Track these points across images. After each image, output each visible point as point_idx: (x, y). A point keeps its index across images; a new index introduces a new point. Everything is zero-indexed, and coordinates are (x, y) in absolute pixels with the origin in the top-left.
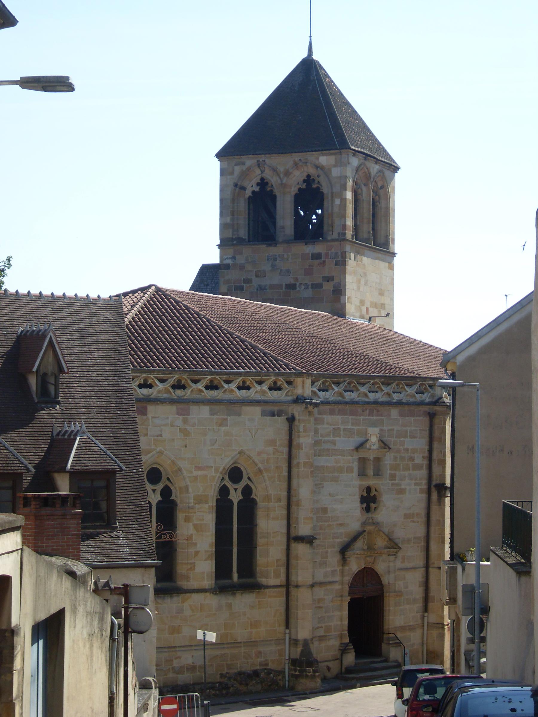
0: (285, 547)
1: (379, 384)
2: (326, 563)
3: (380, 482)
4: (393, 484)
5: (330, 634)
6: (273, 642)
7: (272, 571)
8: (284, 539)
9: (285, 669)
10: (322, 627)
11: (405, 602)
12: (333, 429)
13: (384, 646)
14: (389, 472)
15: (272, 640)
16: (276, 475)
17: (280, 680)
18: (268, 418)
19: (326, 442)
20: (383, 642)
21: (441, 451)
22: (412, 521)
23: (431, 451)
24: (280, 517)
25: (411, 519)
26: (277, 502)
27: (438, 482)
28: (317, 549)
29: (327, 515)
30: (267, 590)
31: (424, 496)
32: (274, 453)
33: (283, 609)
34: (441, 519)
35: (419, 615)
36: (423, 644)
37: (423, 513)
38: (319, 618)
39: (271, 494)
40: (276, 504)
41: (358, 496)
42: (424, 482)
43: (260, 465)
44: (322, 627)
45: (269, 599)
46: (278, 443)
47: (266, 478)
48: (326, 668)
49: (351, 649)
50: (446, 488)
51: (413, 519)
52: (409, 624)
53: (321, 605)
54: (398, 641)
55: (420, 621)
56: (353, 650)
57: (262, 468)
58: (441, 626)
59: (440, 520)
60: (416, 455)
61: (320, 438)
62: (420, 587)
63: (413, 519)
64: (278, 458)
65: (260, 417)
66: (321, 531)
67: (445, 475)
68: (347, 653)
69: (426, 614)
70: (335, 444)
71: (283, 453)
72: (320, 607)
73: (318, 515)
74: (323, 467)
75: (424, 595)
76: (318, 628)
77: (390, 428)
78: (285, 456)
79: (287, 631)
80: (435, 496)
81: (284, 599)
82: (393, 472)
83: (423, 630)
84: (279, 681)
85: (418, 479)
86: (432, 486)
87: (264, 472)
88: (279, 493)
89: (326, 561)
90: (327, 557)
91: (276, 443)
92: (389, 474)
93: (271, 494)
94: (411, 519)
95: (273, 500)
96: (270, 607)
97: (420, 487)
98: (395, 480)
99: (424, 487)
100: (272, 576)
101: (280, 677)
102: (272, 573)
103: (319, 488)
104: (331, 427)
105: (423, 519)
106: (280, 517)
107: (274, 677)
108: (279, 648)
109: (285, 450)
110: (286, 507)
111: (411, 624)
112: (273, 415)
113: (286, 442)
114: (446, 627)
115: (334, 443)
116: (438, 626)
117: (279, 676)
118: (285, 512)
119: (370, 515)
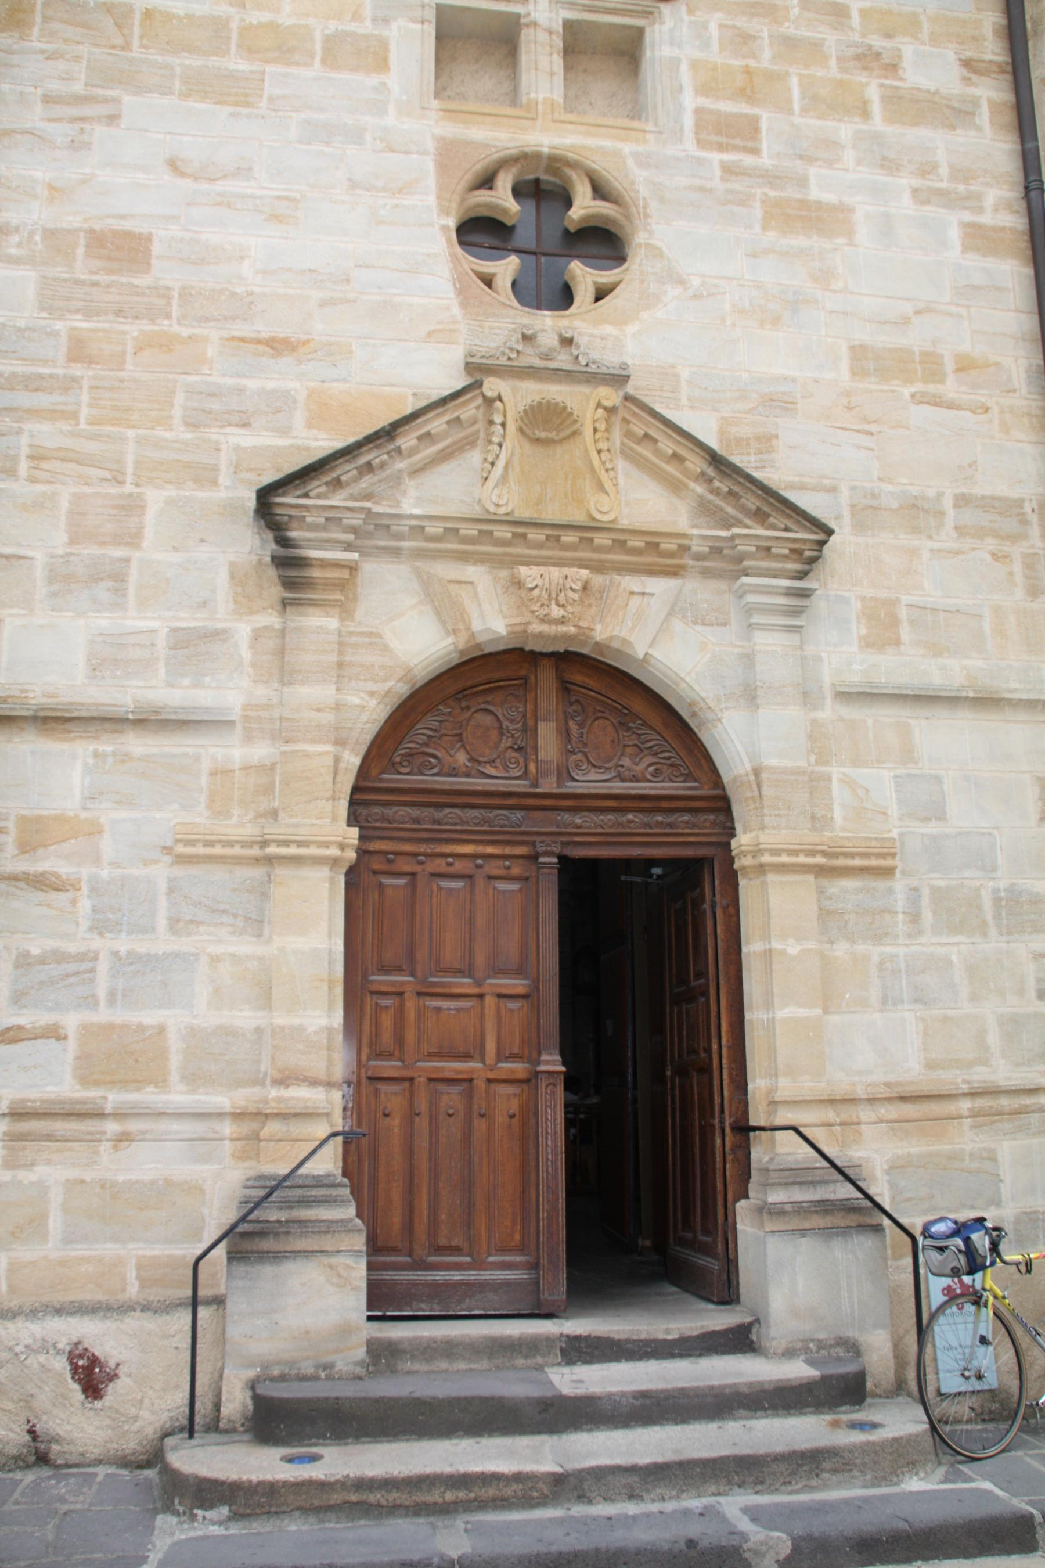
2: (118, 578)
3: (627, 148)
4: (728, 170)
5: (149, 1096)
10: (55, 1033)
11: (927, 916)
14: (690, 101)
22: (937, 402)
25: (918, 387)
28: (32, 480)
29: (142, 281)
41: (432, 200)
44: (55, 1033)
48: (61, 1365)
49: (329, 1228)
51: (931, 388)
54: (845, 1191)
56: (360, 1242)
63: (931, 388)
66: (78, 370)
68: (277, 1257)
73: (60, 271)
82: (727, 107)
85: (944, 171)
89: (127, 560)
90: (133, 539)
92: (698, 111)
94: (918, 387)
97: (968, 217)
98: (755, 151)
103: (82, 119)
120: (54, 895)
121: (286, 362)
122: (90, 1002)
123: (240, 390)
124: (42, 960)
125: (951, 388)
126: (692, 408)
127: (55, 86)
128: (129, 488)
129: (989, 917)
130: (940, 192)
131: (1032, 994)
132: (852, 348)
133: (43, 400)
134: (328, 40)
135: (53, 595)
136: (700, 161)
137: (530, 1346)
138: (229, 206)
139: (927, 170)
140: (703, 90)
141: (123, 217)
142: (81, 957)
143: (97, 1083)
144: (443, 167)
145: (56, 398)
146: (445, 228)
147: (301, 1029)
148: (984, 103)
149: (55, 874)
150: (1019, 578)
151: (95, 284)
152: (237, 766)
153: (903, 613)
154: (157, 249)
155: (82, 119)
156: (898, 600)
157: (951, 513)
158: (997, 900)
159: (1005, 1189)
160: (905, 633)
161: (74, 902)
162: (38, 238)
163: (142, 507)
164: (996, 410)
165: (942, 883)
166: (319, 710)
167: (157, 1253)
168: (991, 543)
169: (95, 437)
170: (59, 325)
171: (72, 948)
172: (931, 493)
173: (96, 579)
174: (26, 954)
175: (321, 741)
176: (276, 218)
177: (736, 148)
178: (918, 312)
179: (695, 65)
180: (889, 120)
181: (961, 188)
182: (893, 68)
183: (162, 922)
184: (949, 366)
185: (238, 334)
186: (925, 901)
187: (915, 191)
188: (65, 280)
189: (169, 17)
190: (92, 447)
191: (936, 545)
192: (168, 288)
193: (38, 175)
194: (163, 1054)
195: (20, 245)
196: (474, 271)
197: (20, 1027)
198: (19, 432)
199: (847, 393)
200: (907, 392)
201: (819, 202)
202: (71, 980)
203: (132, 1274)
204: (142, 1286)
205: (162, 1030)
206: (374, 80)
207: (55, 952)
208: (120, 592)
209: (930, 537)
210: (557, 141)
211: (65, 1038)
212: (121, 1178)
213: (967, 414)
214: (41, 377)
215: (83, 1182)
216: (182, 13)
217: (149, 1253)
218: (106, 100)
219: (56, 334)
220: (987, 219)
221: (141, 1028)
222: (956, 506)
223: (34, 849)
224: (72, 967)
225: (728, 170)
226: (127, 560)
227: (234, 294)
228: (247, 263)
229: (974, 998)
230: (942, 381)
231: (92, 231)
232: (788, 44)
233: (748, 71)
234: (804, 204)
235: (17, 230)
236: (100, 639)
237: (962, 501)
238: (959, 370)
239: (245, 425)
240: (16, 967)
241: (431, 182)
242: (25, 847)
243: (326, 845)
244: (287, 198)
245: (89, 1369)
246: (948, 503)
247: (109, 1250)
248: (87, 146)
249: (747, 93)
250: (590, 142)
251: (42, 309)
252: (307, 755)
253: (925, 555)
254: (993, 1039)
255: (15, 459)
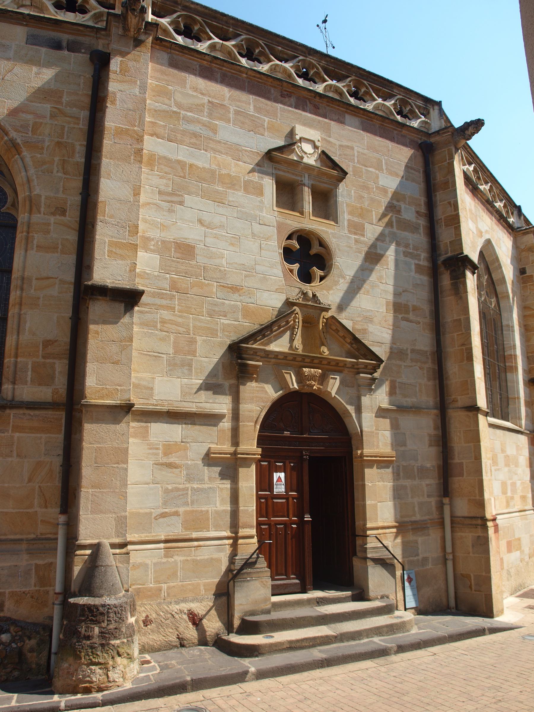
0: (69, 313)
1: (318, 69)
2: (190, 365)
3: (330, 231)
6: (24, 546)
7: (30, 366)
8: (69, 296)
9: (51, 618)
10: (176, 514)
11: (401, 474)
12: (209, 101)
13: (356, 562)
15: (22, 540)
16: (56, 159)
17: (31, 650)
18: (44, 50)
19: (189, 121)
20: (355, 554)
21: (449, 203)
22: (407, 320)
23: (430, 205)
24: (60, 247)
25: (403, 315)
26: (53, 214)
27: (449, 254)
30: (12, 413)
31: (425, 279)
32: (53, 116)
33: (57, 462)
34: (462, 317)
35: (433, 501)
36: (445, 560)
37: (426, 308)
38: (167, 491)
39: (39, 196)
40: (52, 219)
42: (424, 255)
43: (13, 134)
44: (176, 514)
45: (17, 435)
46: (65, 99)
47: (28, 160)
48: (185, 617)
50: (466, 261)
51: (406, 316)
52: (413, 519)
53: (172, 459)
55: (435, 515)
57: (19, 141)
58: (479, 522)
59: (460, 320)
60: (403, 206)
61: (175, 109)
62: (430, 445)
63: (406, 316)
64: (64, 127)
65: (23, 44)
67: (461, 240)
69: (446, 500)
70: (216, 134)
71: (78, 119)
72: (170, 466)
74: (179, 162)
75: (441, 463)
76: (163, 515)
77: (345, 143)
78: (83, 125)
79: (62, 519)
80: (446, 280)
81: (61, 437)
82: (356, 219)
83: (444, 532)
84: (29, 655)
85: (411, 246)
86: (439, 262)
87: (24, 149)
88: (61, 195)
89: (192, 360)
90: (193, 353)
91: (61, 97)
93: (39, 196)
95: (42, 209)
96: (18, 456)
97: (417, 262)
98: (363, 236)
99: (425, 263)
100: (29, 379)
101: (31, 643)
102: (29, 373)
103: (172, 202)
104: (206, 99)
105: (426, 319)
106: (60, 247)
107: (13, 640)
108: (41, 562)
109: (84, 114)
110: (77, 226)
111: (418, 517)
112: (57, 46)
113: (87, 101)
114: (490, 524)
115: (215, 130)
116: (474, 522)
117: (30, 638)
118: (73, 237)
119: (309, 289)
120: (174, 470)
121: (236, 296)
122: (186, 504)
123: (224, 304)
124: (172, 491)
125: (411, 316)
126: (346, 319)
127: (162, 188)
128: (192, 336)
129: (416, 474)
130: (410, 253)
131: (426, 496)
132: (387, 302)
133: (164, 302)
134: (245, 182)
135: (171, 370)
136: (349, 237)
137: (309, 602)
138: (218, 239)
139: (407, 246)
140: (350, 213)
141: (186, 239)
142: (183, 489)
143: (189, 529)
144: (279, 232)
145: (168, 302)
146: (279, 253)
147: (247, 510)
148: (421, 225)
149: (175, 463)
150: (425, 375)
151: (178, 262)
152: (226, 429)
153: (397, 384)
154: (197, 251)
155: (172, 202)
156: (396, 381)
157: (410, 354)
158: (418, 469)
159: (420, 551)
160: (398, 392)
161: (181, 472)
162: (160, 243)
163: (196, 342)
164: (422, 323)
165: (405, 464)
166: (250, 412)
167: (209, 581)
168: (419, 364)
169: (180, 317)
170: (168, 276)
171: (181, 486)
172: (405, 348)
173: (183, 365)
174: (167, 489)
175: (251, 422)
176: (232, 244)
177: (359, 234)
178: (403, 291)
179: (347, 205)
180: (398, 229)
181: (415, 252)
182: (399, 212)
183: (206, 478)
184: (411, 309)
185: (222, 284)
186: (401, 469)
187: (404, 252)
188: (169, 260)
189: (198, 167)
190: (180, 320)
191: (406, 364)
192: (201, 266)
193: (159, 220)
194: (208, 519)
195: (154, 245)
196: (289, 269)
197: (166, 512)
198: (157, 313)
199: (385, 317)
200: (400, 316)
201: (380, 254)
202: (181, 497)
203: (202, 588)
204: (205, 591)
205: (208, 511)
206: (259, 199)
207: (176, 488)
208: (190, 370)
209: (404, 362)
210: (311, 227)
211: (180, 515)
212: (198, 558)
213: (414, 324)
214: (163, 294)
215: (188, 560)
216: (201, 167)
217: (207, 581)
218: (179, 195)
219: (166, 279)
220: (421, 263)
221: (202, 511)
222: (411, 352)
223: (168, 455)
224: (181, 493)
225: (356, 241)
226: (192, 360)
227: (220, 270)
228: (224, 259)
229: (412, 497)
230: (409, 314)
231: (177, 243)
232: (372, 200)
233: (361, 208)
234: (376, 253)
235: (153, 240)
236: (185, 386)
237: (413, 351)
238: (413, 310)
239: (225, 316)
240: (164, 493)
241: (276, 237)
242: (166, 454)
243: (254, 454)
244: (235, 238)
245: (193, 618)
246: (409, 351)
247: (196, 581)
248: (173, 211)
249: (361, 216)
250: (320, 228)
251: (162, 269)
252: (247, 426)
253: (403, 367)
254: (416, 509)
255: (156, 322)
